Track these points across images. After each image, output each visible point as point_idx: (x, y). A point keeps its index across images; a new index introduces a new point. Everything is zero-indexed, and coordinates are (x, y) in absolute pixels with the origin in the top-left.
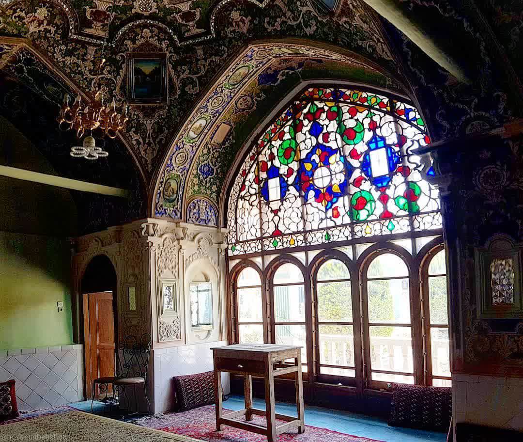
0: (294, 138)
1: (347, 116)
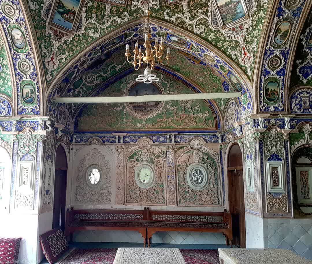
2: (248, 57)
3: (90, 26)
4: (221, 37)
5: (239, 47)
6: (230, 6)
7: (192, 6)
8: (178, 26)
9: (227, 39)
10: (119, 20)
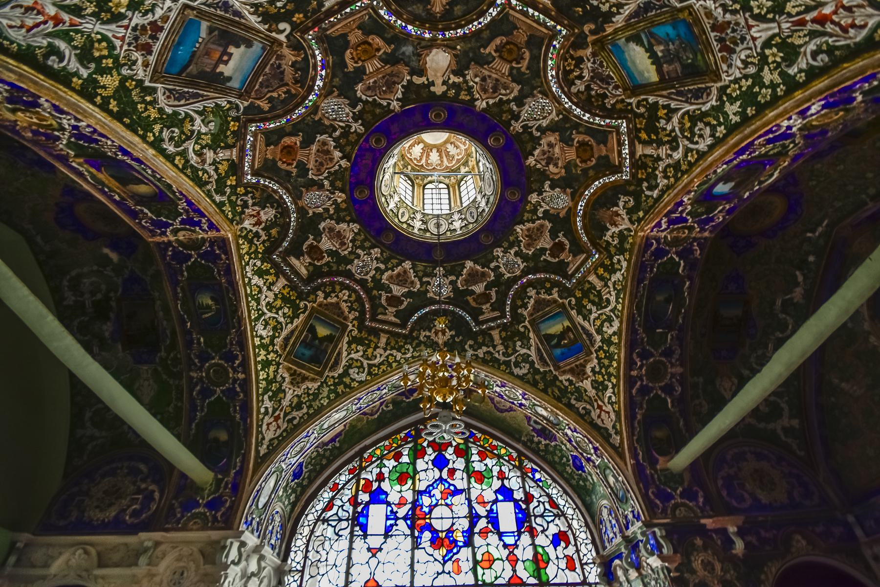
0: (414, 464)
1: (475, 458)
2: (835, 12)
3: (598, 323)
4: (740, 87)
5: (788, 37)
6: (660, 54)
7: (649, 137)
8: (677, 179)
9: (752, 70)
10: (618, 276)
